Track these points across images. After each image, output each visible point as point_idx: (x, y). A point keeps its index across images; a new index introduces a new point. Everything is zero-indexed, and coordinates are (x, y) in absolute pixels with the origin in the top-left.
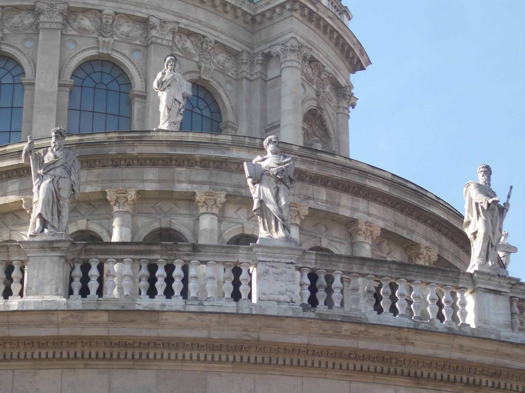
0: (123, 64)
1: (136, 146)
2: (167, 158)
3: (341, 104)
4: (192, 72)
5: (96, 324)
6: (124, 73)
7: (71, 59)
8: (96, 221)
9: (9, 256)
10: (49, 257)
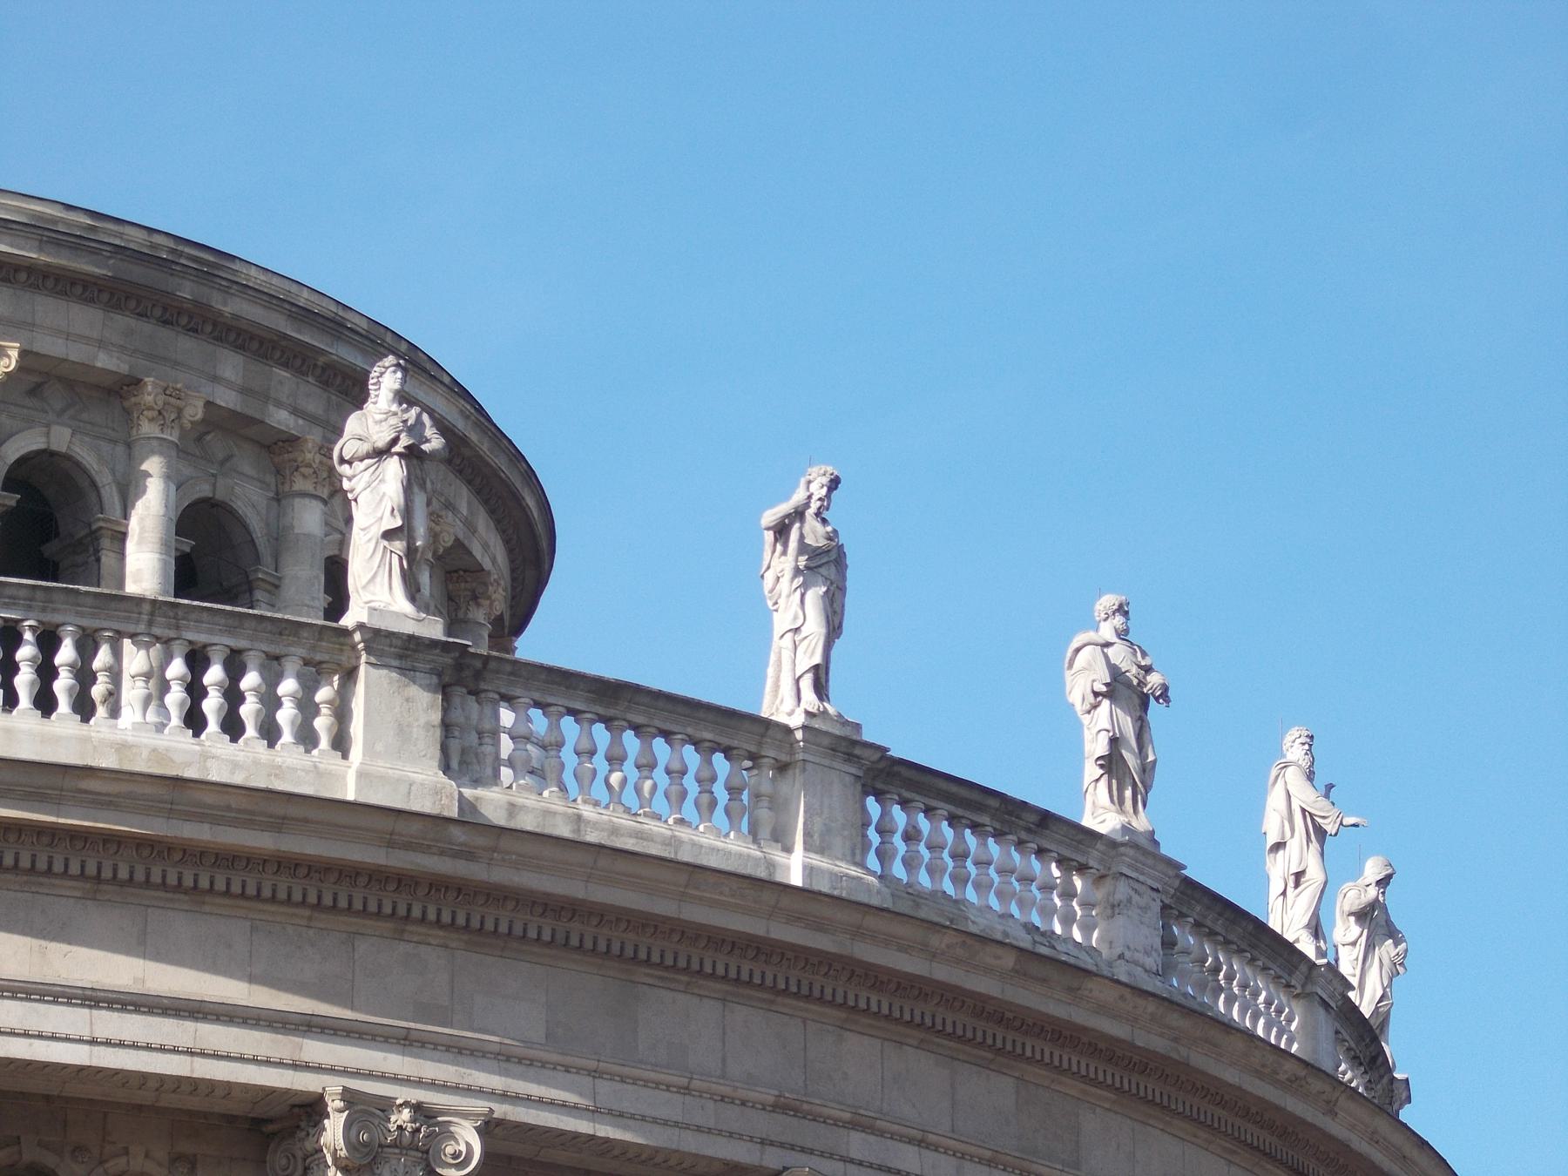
1: (232, 294)
8: (87, 439)
9: (760, 744)
10: (838, 772)
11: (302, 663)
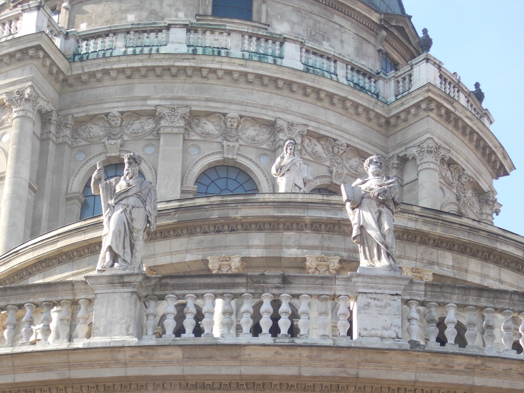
0: (249, 169)
2: (274, 221)
3: (484, 211)
4: (322, 176)
5: (168, 362)
6: (251, 178)
9: (74, 294)
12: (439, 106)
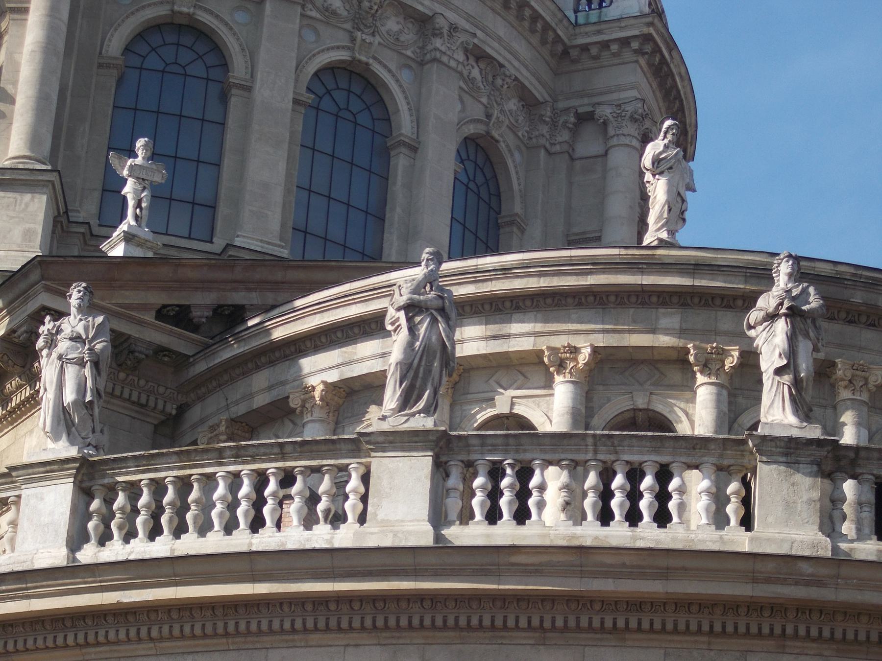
0: (385, 85)
6: (382, 100)
7: (310, 59)
11: (716, 469)
12: (657, 50)
